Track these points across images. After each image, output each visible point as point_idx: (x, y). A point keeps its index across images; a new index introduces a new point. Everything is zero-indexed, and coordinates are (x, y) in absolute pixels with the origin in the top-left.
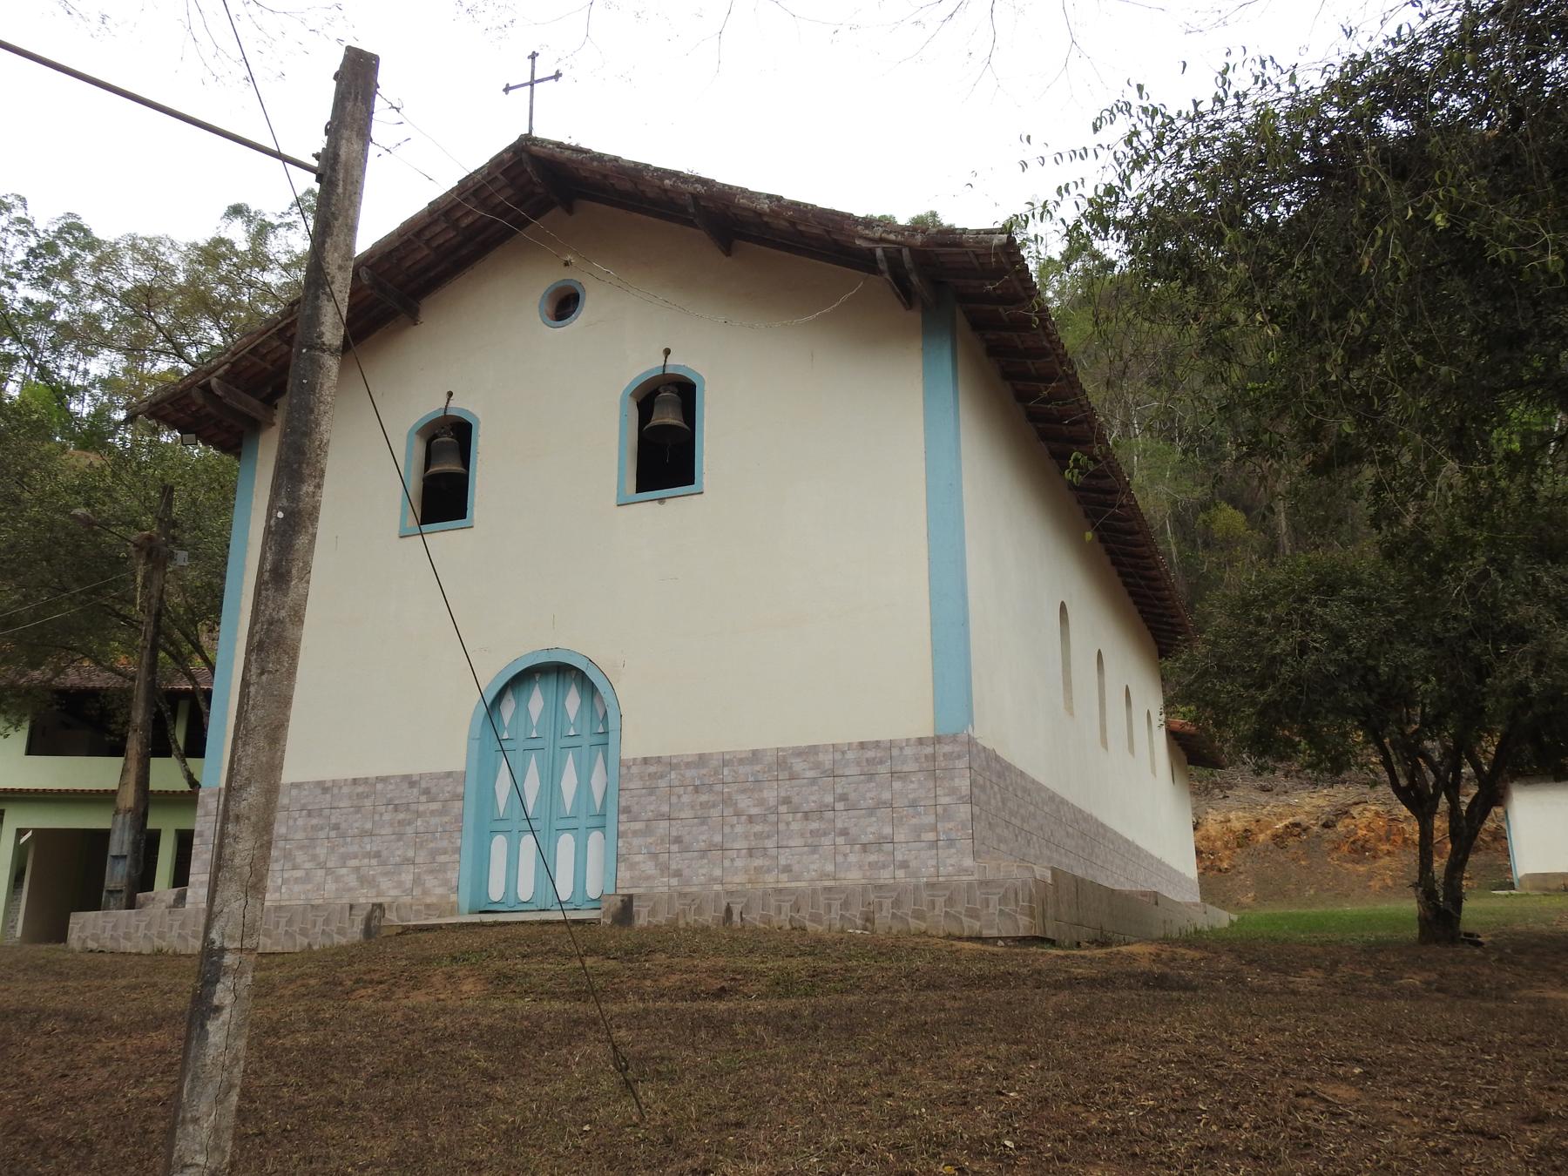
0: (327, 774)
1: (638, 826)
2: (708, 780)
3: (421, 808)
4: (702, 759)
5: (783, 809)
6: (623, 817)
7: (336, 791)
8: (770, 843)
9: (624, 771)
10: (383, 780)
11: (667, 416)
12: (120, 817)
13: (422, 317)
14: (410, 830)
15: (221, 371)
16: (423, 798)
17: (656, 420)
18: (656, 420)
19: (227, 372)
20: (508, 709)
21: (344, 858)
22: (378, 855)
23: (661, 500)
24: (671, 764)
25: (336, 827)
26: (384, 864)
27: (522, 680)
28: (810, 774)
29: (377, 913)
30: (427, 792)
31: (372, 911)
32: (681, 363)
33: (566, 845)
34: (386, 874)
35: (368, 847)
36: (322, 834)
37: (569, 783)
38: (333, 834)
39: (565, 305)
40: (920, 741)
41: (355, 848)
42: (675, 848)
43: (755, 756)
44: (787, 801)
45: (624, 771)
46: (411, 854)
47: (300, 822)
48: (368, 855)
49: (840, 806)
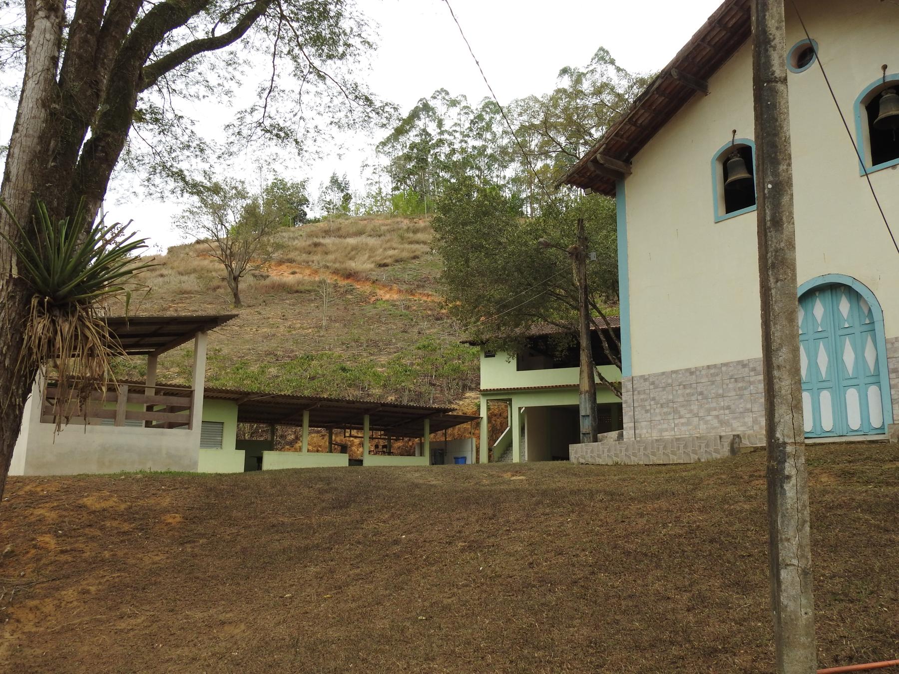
0: (691, 365)
3: (752, 379)
6: (893, 376)
7: (698, 373)
9: (889, 346)
10: (726, 365)
12: (583, 396)
13: (710, 90)
14: (746, 392)
15: (601, 150)
16: (752, 373)
17: (882, 115)
18: (882, 115)
19: (604, 149)
21: (709, 411)
22: (729, 408)
23: (894, 167)
25: (701, 393)
26: (733, 412)
29: (737, 440)
31: (734, 439)
33: (852, 395)
34: (735, 418)
36: (694, 398)
37: (849, 357)
38: (700, 397)
41: (714, 405)
45: (889, 346)
46: (749, 406)
47: (680, 392)
48: (723, 408)
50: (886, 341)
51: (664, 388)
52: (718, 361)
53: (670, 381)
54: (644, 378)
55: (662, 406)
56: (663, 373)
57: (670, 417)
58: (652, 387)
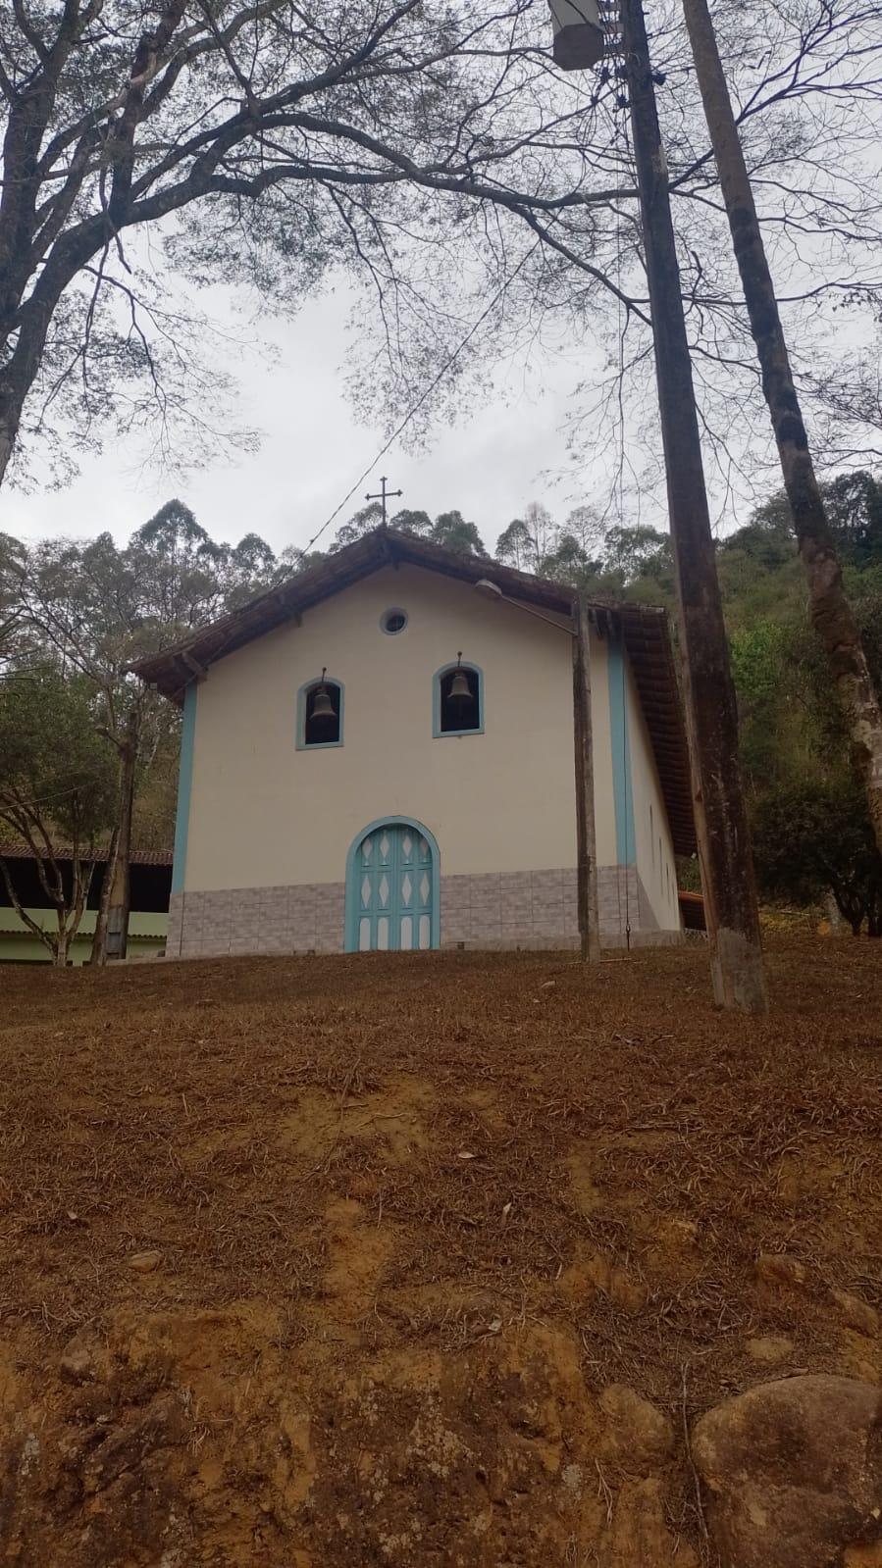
0: (256, 884)
1: (452, 911)
2: (493, 887)
3: (319, 903)
4: (488, 876)
5: (535, 902)
6: (443, 907)
8: (528, 920)
10: (294, 887)
11: (460, 690)
15: (189, 649)
20: (367, 849)
22: (292, 929)
23: (460, 736)
24: (471, 879)
25: (264, 914)
27: (376, 833)
28: (550, 884)
30: (321, 894)
32: (470, 660)
33: (406, 923)
35: (285, 925)
37: (407, 890)
38: (262, 918)
39: (395, 623)
40: (610, 868)
42: (474, 923)
43: (519, 875)
44: (537, 898)
46: (313, 928)
49: (566, 901)
50: (441, 878)
51: (222, 907)
52: (286, 883)
53: (230, 899)
54: (199, 895)
55: (217, 925)
56: (223, 891)
57: (226, 937)
58: (207, 905)
